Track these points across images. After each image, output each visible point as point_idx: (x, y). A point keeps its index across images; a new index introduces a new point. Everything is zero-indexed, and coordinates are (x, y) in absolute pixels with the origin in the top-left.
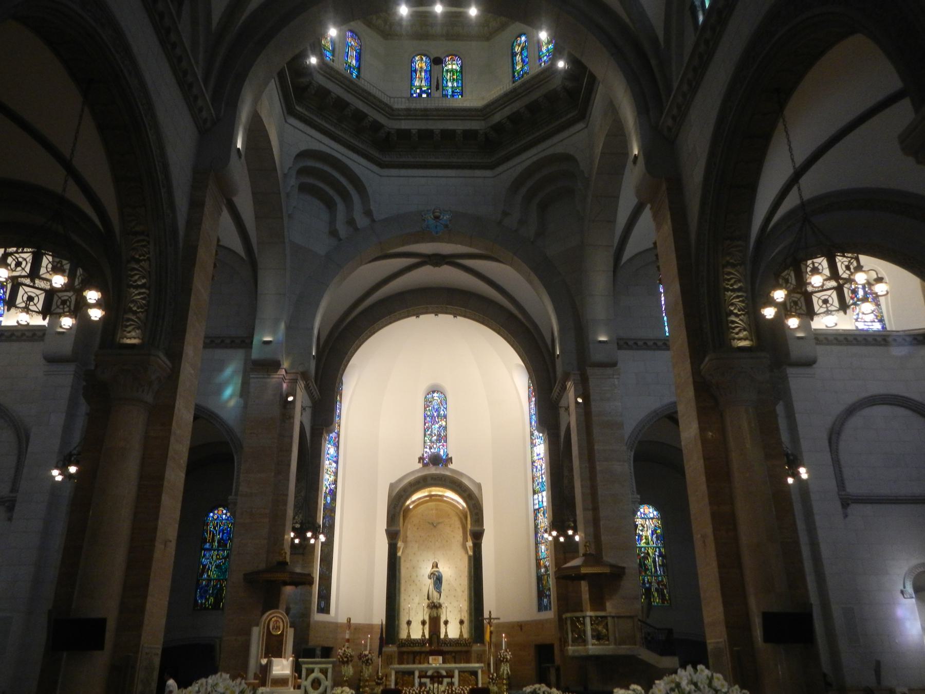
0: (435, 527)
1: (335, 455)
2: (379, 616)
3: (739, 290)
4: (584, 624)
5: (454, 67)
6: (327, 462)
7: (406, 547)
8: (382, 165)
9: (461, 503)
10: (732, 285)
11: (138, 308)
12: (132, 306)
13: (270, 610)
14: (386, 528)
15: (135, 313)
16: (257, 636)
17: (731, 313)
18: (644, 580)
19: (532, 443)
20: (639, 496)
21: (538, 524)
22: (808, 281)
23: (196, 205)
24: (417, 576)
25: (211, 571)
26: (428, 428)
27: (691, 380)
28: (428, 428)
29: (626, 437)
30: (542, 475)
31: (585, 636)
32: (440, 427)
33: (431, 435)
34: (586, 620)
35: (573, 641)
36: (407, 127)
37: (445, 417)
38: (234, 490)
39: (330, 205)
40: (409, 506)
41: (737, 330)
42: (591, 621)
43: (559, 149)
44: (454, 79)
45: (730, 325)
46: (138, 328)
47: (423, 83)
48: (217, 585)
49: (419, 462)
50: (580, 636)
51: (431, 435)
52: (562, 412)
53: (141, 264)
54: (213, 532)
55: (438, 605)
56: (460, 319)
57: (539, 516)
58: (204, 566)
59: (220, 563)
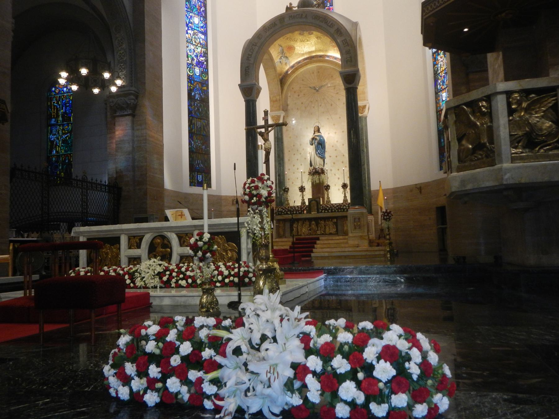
0: (317, 91)
1: (202, 25)
4: (490, 114)
7: (287, 116)
14: (240, 83)
21: (438, 68)
24: (301, 145)
25: (59, 146)
31: (491, 141)
34: (493, 103)
35: (460, 160)
40: (287, 72)
42: (509, 104)
48: (65, 160)
50: (479, 146)
54: (57, 107)
55: (320, 171)
57: (439, 58)
58: (52, 142)
59: (66, 137)
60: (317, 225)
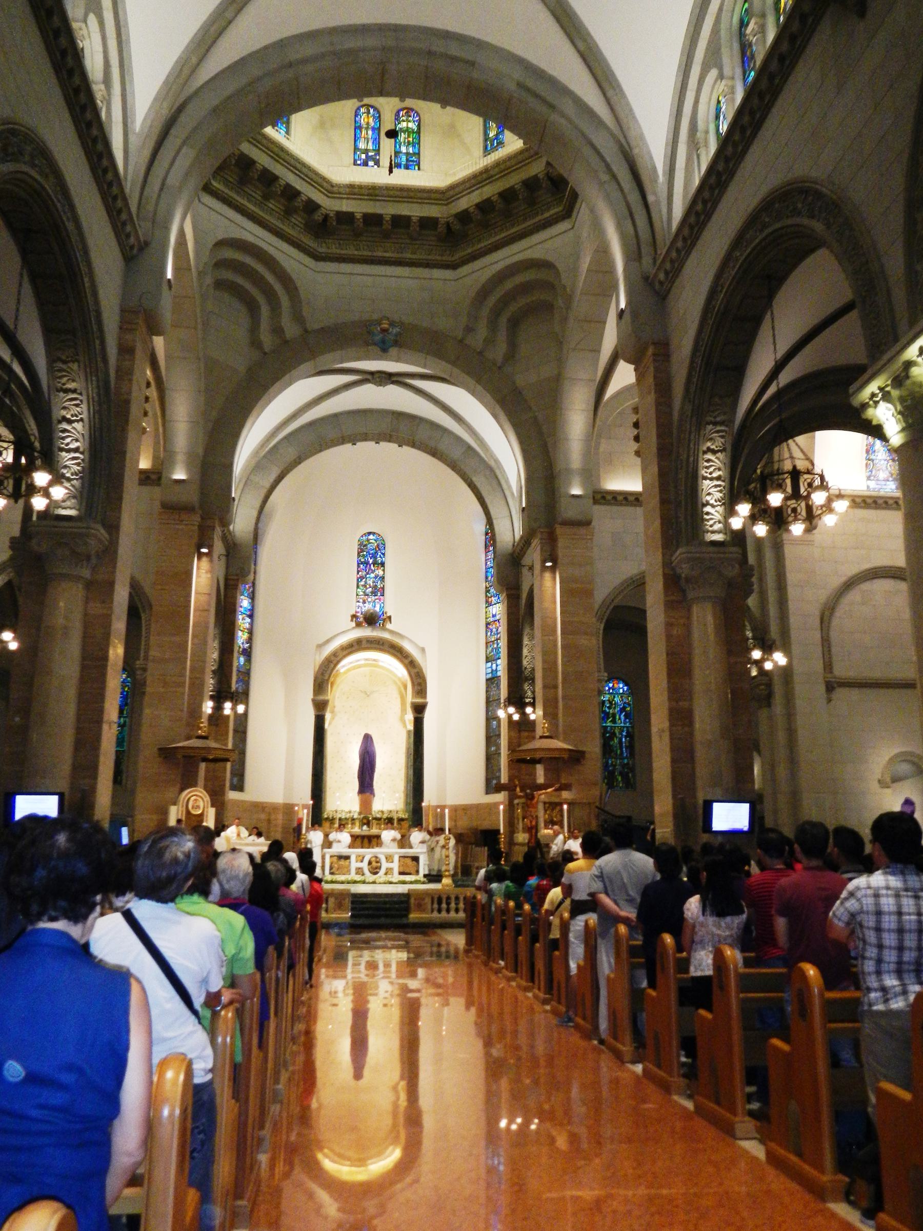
3: (718, 478)
5: (411, 125)
6: (240, 617)
8: (317, 257)
9: (400, 670)
10: (711, 473)
11: (72, 475)
12: (65, 471)
13: (188, 788)
15: (69, 480)
17: (708, 504)
18: (607, 763)
19: (487, 602)
20: (606, 674)
23: (126, 351)
26: (362, 578)
27: (661, 572)
28: (362, 578)
29: (597, 606)
30: (497, 640)
32: (376, 577)
33: (365, 586)
36: (350, 210)
37: (383, 564)
38: (142, 655)
39: (252, 308)
41: (711, 522)
43: (536, 254)
44: (409, 142)
45: (706, 517)
46: (74, 497)
47: (370, 146)
49: (352, 620)
52: (525, 571)
53: (73, 425)
56: (406, 449)
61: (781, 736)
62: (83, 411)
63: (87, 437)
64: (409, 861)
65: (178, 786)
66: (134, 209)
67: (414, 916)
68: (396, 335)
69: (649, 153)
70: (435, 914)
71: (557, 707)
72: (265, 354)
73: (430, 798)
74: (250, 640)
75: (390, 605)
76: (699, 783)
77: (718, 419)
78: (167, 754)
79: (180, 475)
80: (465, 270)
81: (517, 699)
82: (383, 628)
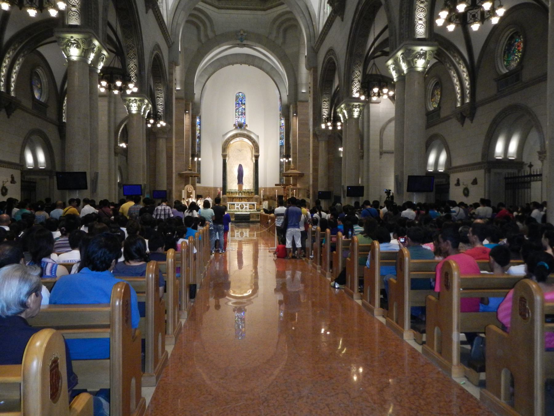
2: (220, 184)
3: (327, 108)
4: (289, 190)
9: (250, 143)
14: (221, 153)
16: (184, 193)
17: (324, 115)
22: (446, 7)
23: (171, 74)
26: (237, 109)
28: (237, 109)
32: (242, 109)
33: (238, 112)
37: (244, 104)
39: (198, 28)
51: (238, 112)
56: (251, 66)
60: (242, 199)
61: (365, 168)
62: (163, 95)
63: (164, 101)
64: (252, 205)
65: (184, 184)
66: (170, 34)
67: (251, 220)
68: (246, 36)
69: (314, 10)
70: (257, 219)
71: (296, 159)
72: (203, 44)
73: (261, 185)
74: (200, 133)
75: (248, 120)
76: (319, 187)
77: (327, 93)
78: (180, 175)
79: (178, 88)
80: (269, 11)
81: (287, 156)
82: (245, 129)
